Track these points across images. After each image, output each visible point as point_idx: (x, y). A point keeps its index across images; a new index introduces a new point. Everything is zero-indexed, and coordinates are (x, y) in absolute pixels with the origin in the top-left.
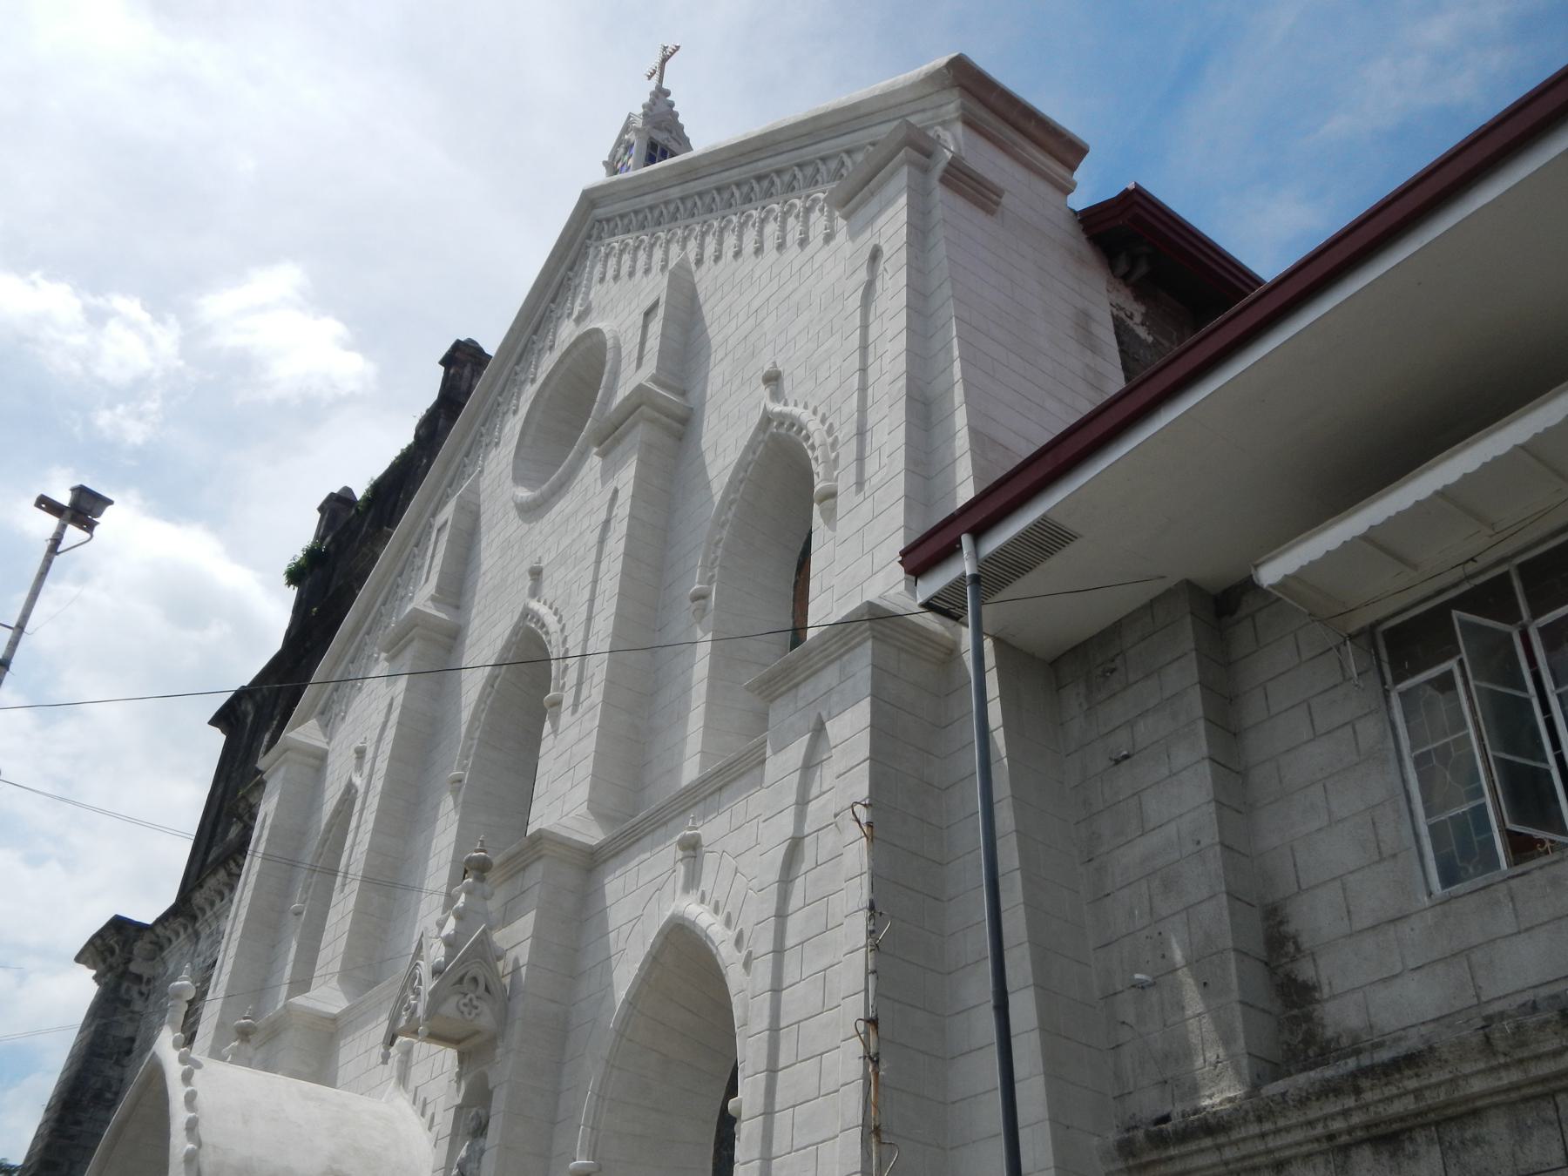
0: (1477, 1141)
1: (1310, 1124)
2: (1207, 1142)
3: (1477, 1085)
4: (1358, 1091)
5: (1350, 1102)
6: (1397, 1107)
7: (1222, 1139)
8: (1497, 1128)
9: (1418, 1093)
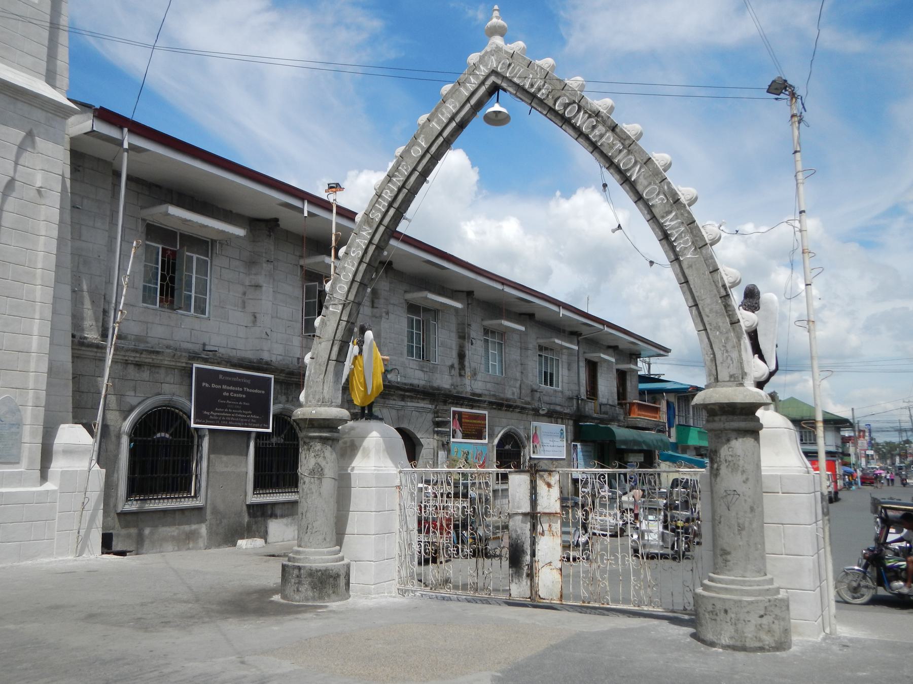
0: (158, 373)
1: (125, 356)
2: (95, 350)
3: (166, 363)
4: (141, 353)
5: (138, 355)
6: (147, 360)
7: (99, 351)
8: (162, 371)
9: (153, 359)
